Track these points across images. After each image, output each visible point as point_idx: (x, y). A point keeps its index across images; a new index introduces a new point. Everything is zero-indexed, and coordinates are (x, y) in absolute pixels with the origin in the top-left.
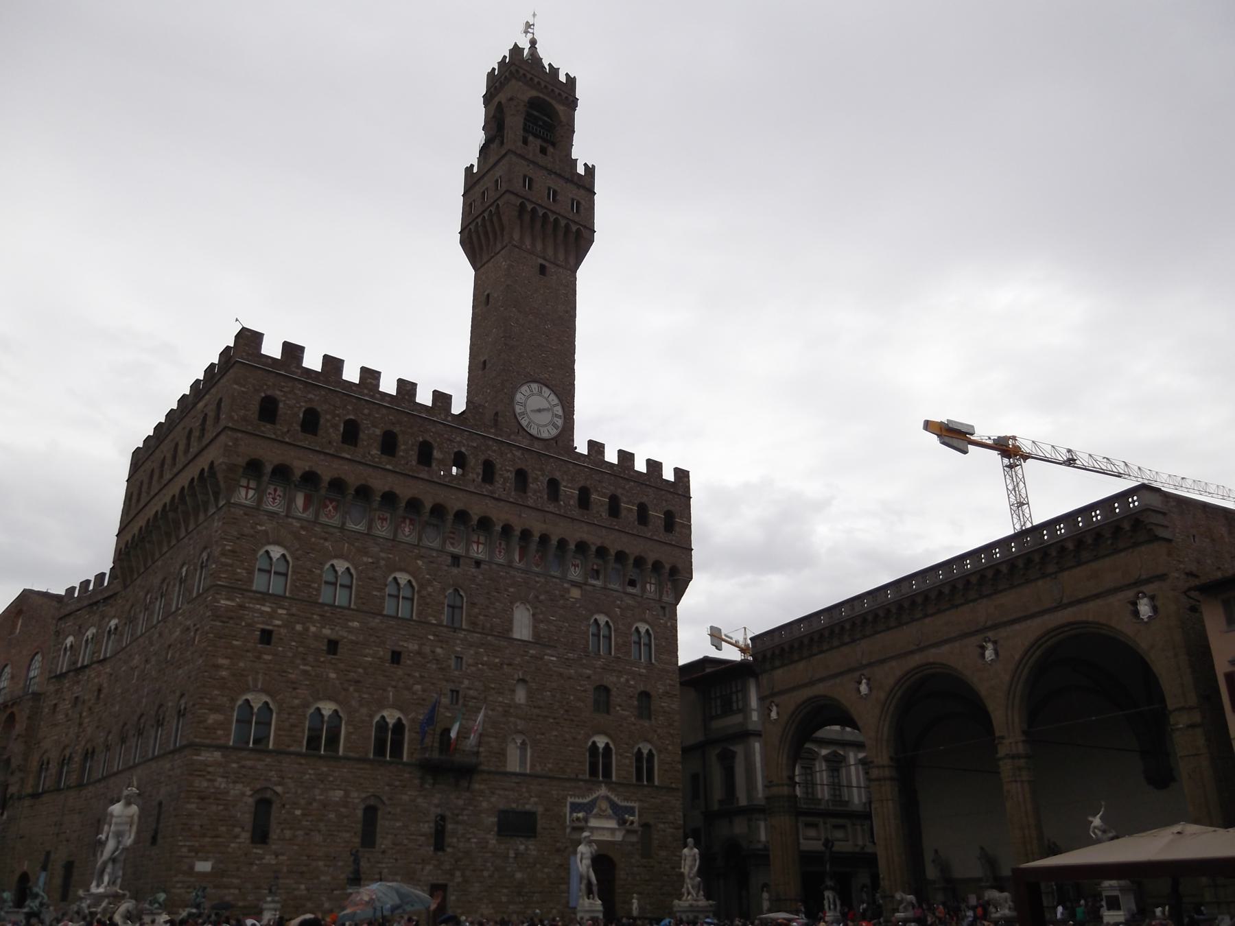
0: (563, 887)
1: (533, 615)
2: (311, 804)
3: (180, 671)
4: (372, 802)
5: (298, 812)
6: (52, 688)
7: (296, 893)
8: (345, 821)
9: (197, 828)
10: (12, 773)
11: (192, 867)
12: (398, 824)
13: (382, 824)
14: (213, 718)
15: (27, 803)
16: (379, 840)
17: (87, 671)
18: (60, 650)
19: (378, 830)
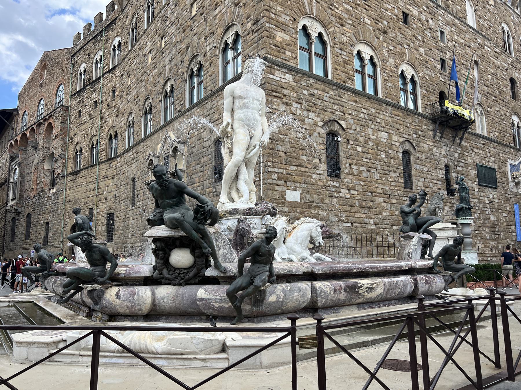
0: (513, 227)
1: (476, 11)
2: (367, 142)
3: (217, 11)
4: (407, 146)
5: (359, 149)
6: (75, 102)
7: (368, 227)
8: (392, 160)
9: (282, 154)
10: (56, 161)
11: (283, 196)
12: (425, 169)
13: (415, 168)
14: (280, 36)
15: (69, 178)
16: (415, 182)
17: (101, 81)
18: (77, 75)
19: (413, 172)
